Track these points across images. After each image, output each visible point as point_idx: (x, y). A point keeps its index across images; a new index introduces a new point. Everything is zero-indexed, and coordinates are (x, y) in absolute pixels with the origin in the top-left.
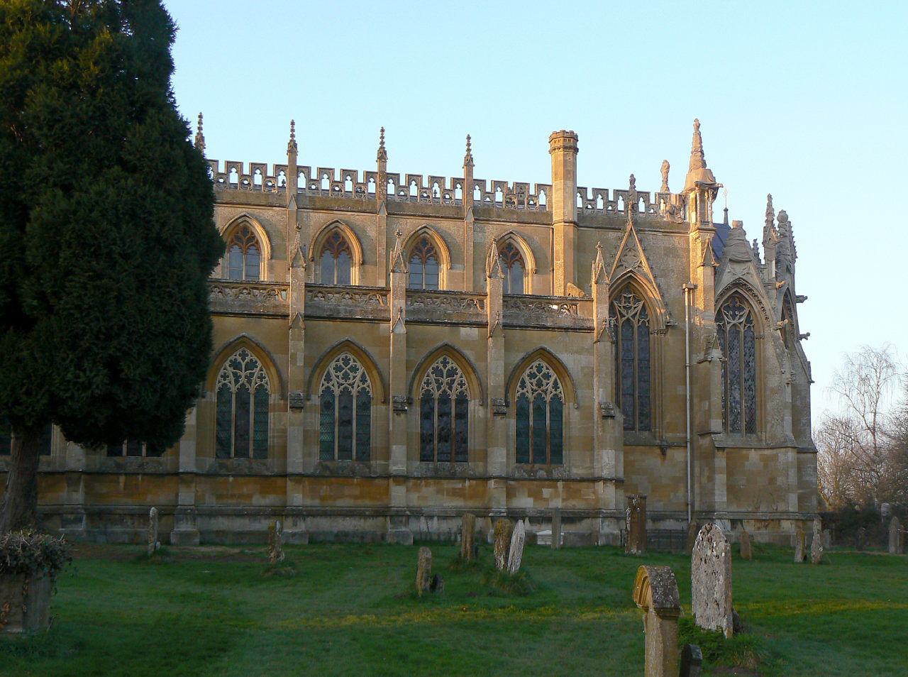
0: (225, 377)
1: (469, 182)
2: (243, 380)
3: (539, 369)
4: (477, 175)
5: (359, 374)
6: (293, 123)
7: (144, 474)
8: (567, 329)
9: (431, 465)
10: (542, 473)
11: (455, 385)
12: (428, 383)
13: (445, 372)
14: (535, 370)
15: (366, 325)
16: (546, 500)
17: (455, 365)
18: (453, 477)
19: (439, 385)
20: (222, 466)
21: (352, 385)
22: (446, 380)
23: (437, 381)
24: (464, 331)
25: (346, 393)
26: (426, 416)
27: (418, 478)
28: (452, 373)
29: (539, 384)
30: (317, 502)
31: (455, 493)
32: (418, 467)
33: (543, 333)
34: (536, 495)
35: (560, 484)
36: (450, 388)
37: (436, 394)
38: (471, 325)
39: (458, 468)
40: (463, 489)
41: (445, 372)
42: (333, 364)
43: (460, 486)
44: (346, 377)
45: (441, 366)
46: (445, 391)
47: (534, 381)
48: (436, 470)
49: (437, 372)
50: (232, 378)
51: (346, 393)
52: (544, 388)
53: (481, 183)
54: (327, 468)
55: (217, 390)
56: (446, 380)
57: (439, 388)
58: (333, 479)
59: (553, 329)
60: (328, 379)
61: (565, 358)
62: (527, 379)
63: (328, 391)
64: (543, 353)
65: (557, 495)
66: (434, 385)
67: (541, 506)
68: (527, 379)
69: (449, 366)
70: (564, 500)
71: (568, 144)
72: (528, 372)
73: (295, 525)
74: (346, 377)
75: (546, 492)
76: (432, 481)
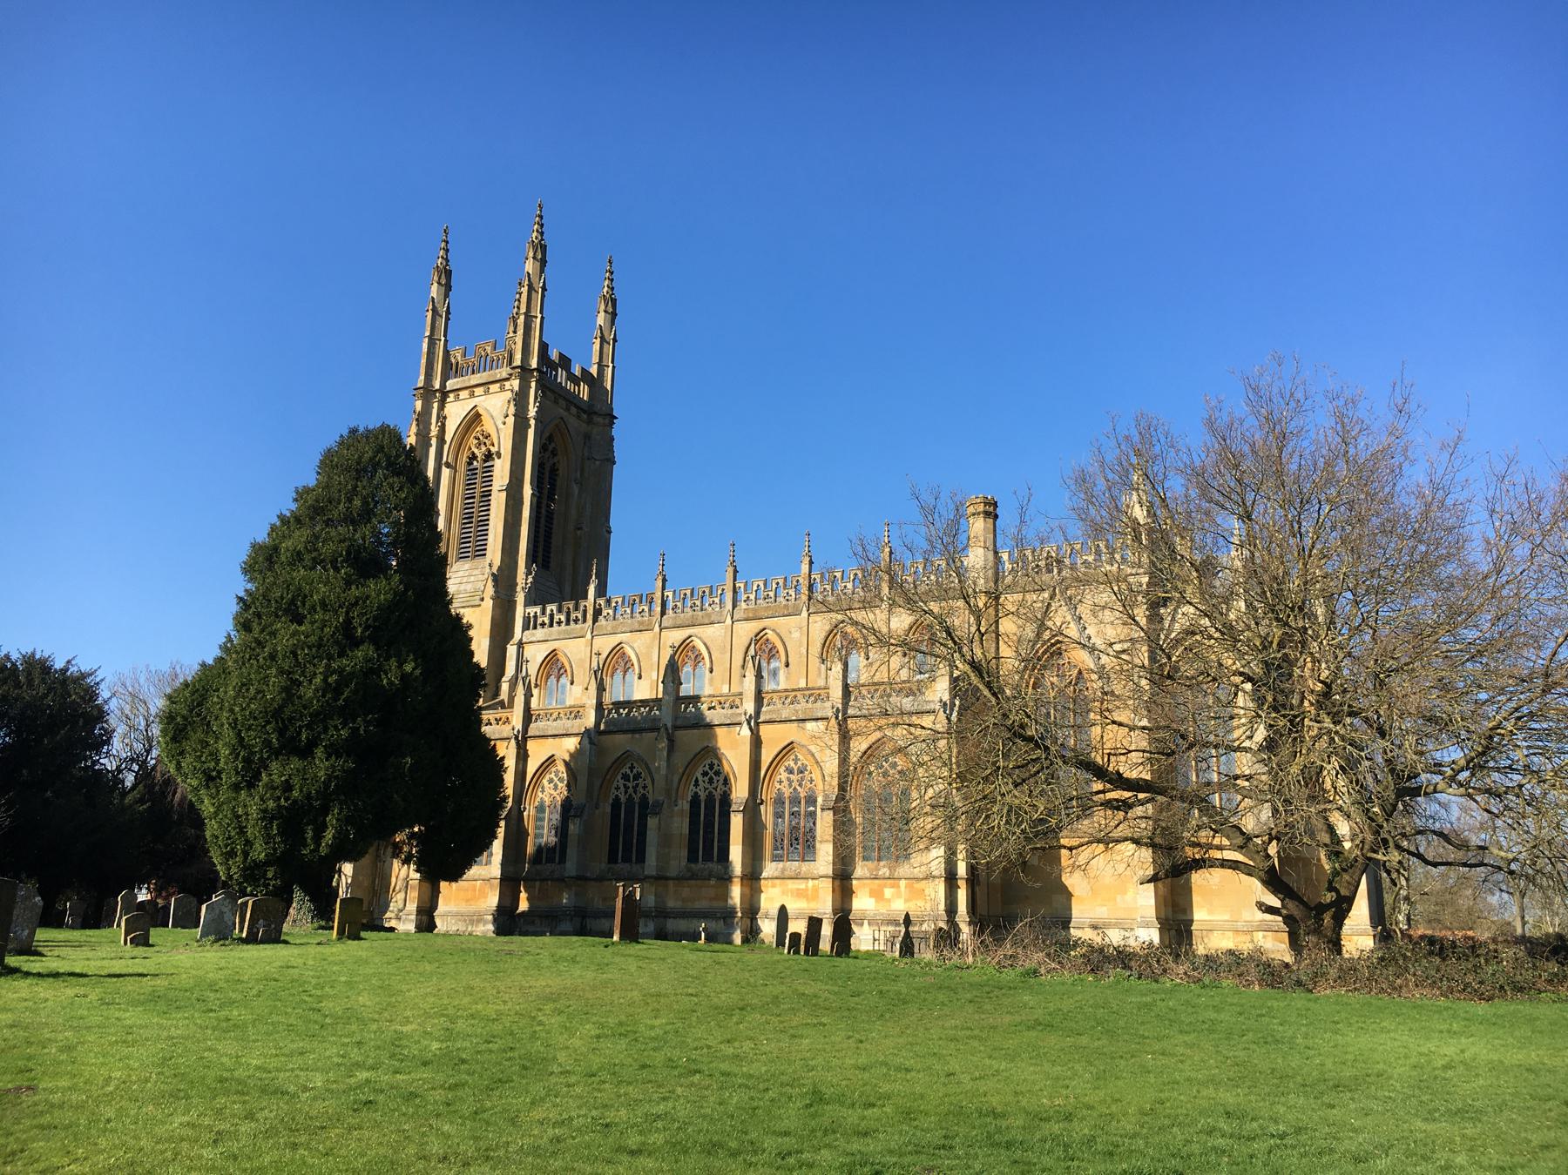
0: (617, 788)
2: (631, 790)
9: (781, 865)
10: (884, 871)
24: (810, 725)
25: (710, 797)
34: (877, 895)
35: (903, 883)
39: (805, 867)
42: (700, 770)
44: (711, 781)
48: (783, 870)
51: (710, 797)
54: (689, 870)
63: (696, 797)
65: (898, 895)
66: (786, 783)
67: (883, 909)
70: (906, 901)
74: (711, 781)
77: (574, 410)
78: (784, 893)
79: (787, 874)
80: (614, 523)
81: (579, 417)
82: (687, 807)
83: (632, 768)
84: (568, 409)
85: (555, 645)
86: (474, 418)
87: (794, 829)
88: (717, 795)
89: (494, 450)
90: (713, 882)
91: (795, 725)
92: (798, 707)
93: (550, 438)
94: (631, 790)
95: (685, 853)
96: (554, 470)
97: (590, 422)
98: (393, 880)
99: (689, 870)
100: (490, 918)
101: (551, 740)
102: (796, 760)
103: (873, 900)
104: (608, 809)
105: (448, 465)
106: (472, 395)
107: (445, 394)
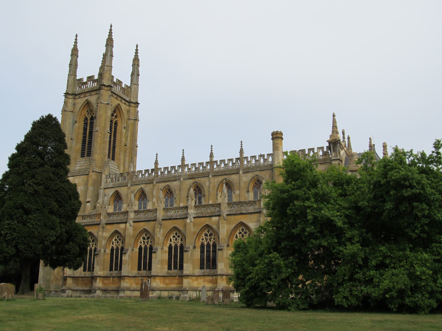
1: (211, 163)
2: (146, 243)
4: (214, 159)
5: (180, 238)
6: (212, 146)
7: (113, 277)
8: (251, 213)
9: (203, 271)
11: (212, 239)
12: (203, 239)
15: (181, 220)
17: (212, 232)
19: (206, 239)
20: (138, 273)
21: (178, 242)
26: (202, 252)
27: (197, 276)
30: (165, 286)
32: (198, 271)
33: (242, 216)
36: (210, 241)
37: (205, 243)
38: (216, 216)
42: (172, 235)
45: (207, 233)
46: (208, 242)
47: (241, 235)
48: (204, 273)
50: (143, 243)
51: (176, 246)
53: (246, 158)
55: (138, 247)
56: (208, 238)
59: (245, 214)
60: (171, 240)
64: (242, 224)
71: (277, 137)
72: (238, 232)
73: (152, 294)
74: (176, 239)
76: (202, 277)
77: (123, 101)
78: (204, 281)
79: (205, 274)
80: (139, 143)
81: (125, 104)
82: (167, 249)
83: (146, 235)
84: (121, 101)
85: (117, 189)
87: (208, 257)
88: (179, 245)
89: (93, 116)
91: (208, 218)
93: (115, 111)
94: (146, 243)
95: (166, 266)
96: (116, 123)
97: (129, 106)
99: (168, 273)
101: (115, 225)
104: (138, 250)
106: (85, 96)
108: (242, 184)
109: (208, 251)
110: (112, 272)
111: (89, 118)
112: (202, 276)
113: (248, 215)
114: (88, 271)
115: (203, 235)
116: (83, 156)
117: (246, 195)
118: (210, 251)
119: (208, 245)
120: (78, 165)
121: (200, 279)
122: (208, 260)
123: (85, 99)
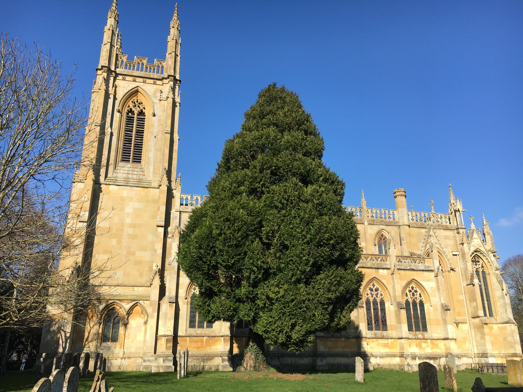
3: (413, 288)
9: (373, 332)
13: (374, 289)
14: (411, 289)
16: (424, 349)
17: (378, 287)
18: (383, 338)
22: (374, 293)
23: (371, 294)
24: (381, 271)
26: (368, 309)
28: (377, 290)
29: (413, 294)
30: (327, 350)
31: (386, 346)
34: (419, 346)
35: (429, 341)
36: (377, 297)
37: (371, 299)
39: (385, 333)
40: (388, 343)
41: (374, 289)
43: (386, 342)
45: (372, 287)
47: (411, 293)
49: (371, 290)
52: (415, 296)
57: (372, 297)
58: (333, 339)
61: (423, 283)
62: (408, 293)
65: (428, 346)
66: (370, 295)
68: (408, 293)
69: (375, 287)
70: (431, 349)
72: (408, 290)
73: (322, 361)
75: (424, 345)
76: (374, 340)
78: (378, 345)
79: (378, 336)
86: (135, 92)
87: (376, 315)
90: (343, 339)
91: (374, 270)
92: (374, 262)
98: (86, 334)
100: (226, 358)
102: (374, 285)
103: (418, 348)
105: (119, 111)
107: (117, 75)
108: (368, 237)
109: (376, 309)
110: (242, 330)
111: (136, 112)
112: (374, 338)
113: (419, 272)
114: (416, 331)
115: (368, 289)
116: (125, 159)
117: (373, 249)
118: (378, 309)
119: (375, 303)
120: (121, 171)
121: (373, 342)
122: (377, 320)
123: (133, 85)
